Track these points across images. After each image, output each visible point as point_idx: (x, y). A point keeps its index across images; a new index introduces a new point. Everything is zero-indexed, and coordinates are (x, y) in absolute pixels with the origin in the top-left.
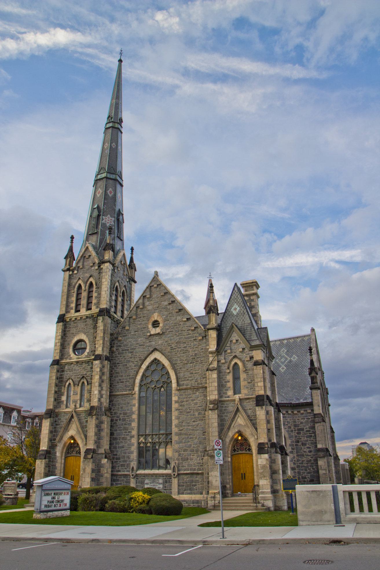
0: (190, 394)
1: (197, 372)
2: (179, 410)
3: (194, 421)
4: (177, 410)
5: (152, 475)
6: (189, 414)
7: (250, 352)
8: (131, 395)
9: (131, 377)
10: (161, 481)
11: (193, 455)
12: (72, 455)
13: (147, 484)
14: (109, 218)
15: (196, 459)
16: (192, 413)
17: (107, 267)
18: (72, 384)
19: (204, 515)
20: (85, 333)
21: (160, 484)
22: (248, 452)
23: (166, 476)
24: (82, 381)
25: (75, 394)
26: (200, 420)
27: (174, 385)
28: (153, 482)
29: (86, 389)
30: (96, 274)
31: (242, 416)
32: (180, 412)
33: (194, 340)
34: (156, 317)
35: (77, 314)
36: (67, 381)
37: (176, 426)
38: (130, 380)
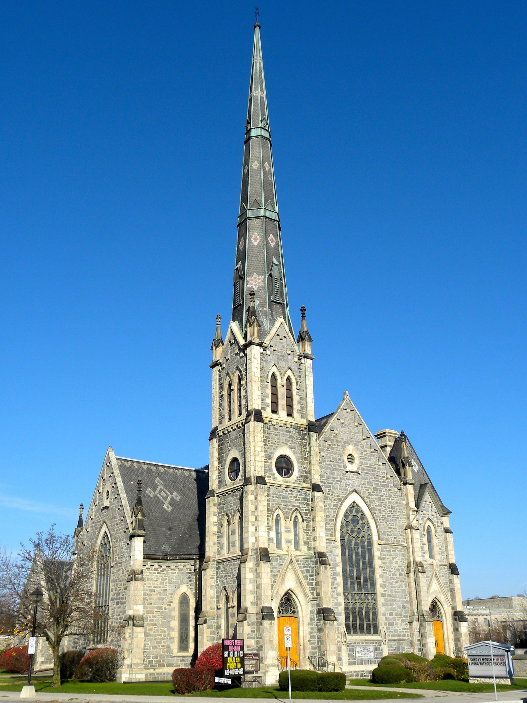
0: (390, 551)
1: (395, 527)
2: (382, 567)
3: (396, 582)
4: (380, 567)
5: (362, 642)
6: (391, 573)
7: (441, 518)
8: (333, 542)
9: (330, 518)
10: (372, 648)
11: (398, 620)
12: (289, 614)
13: (358, 652)
14: (259, 283)
15: (401, 625)
16: (393, 572)
17: (255, 351)
18: (282, 515)
19: (51, 693)
20: (291, 448)
21: (371, 652)
22: (292, 615)
23: (376, 643)
24: (295, 514)
25: (288, 531)
26: (401, 581)
27: (375, 538)
28: (365, 650)
29: (301, 526)
30: (295, 367)
31: (295, 571)
32: (383, 570)
33: (389, 490)
34: (350, 449)
35: (274, 416)
36: (275, 511)
37: (381, 586)
38: (330, 523)
